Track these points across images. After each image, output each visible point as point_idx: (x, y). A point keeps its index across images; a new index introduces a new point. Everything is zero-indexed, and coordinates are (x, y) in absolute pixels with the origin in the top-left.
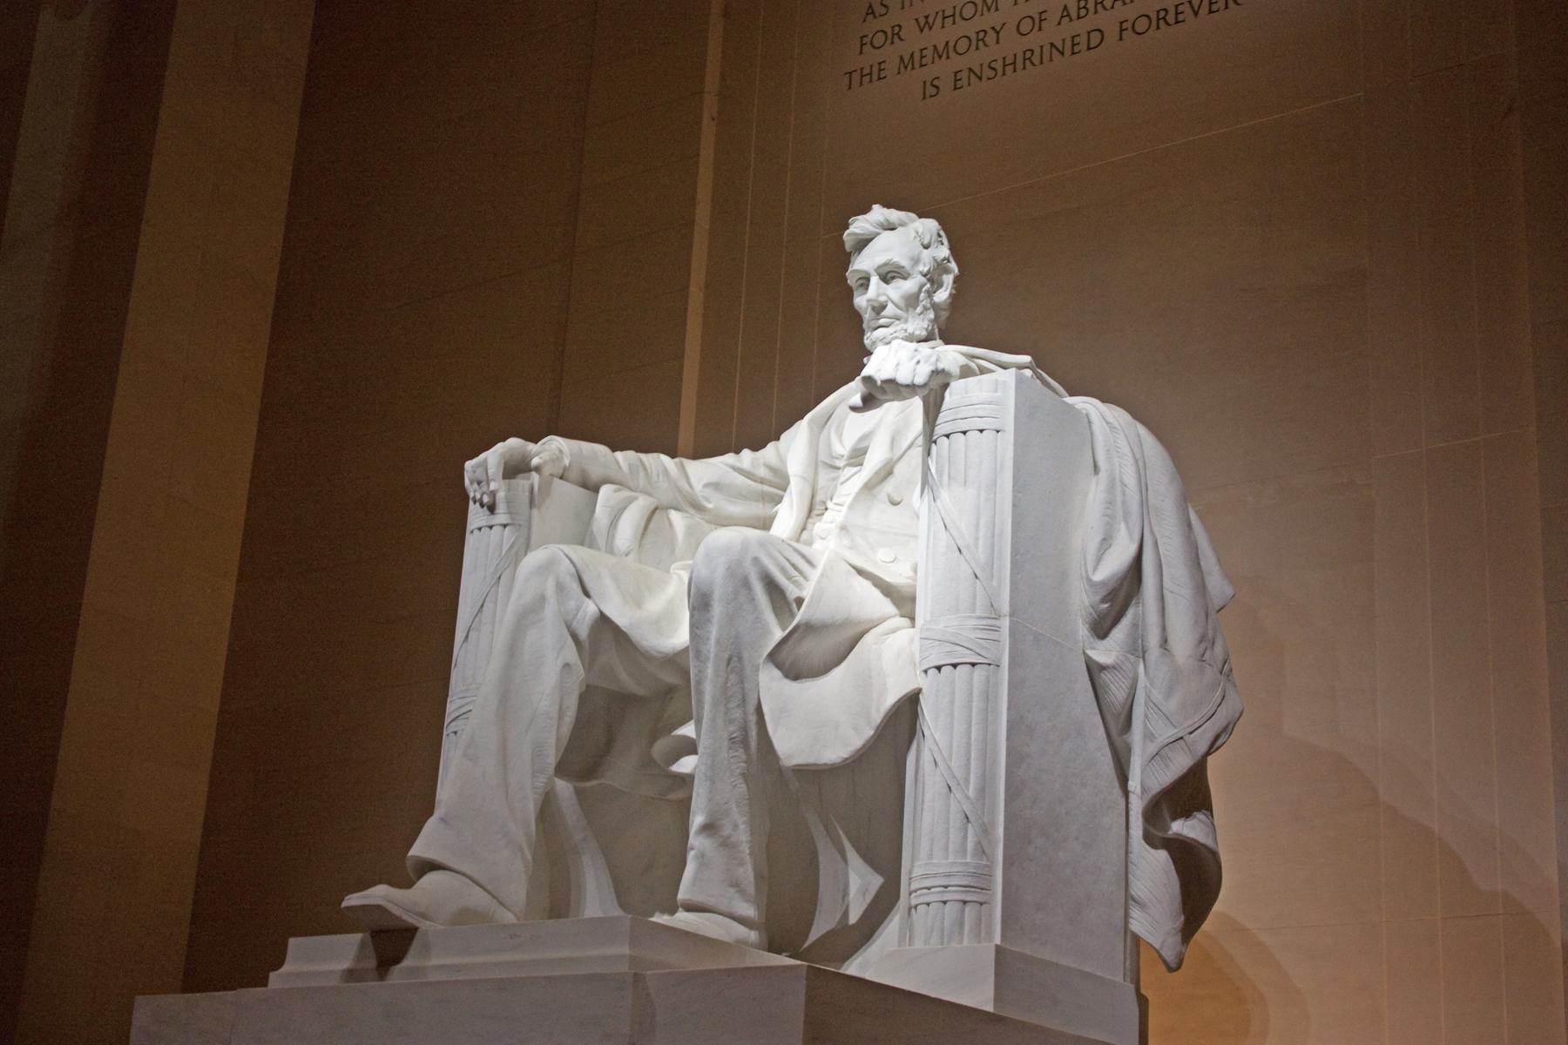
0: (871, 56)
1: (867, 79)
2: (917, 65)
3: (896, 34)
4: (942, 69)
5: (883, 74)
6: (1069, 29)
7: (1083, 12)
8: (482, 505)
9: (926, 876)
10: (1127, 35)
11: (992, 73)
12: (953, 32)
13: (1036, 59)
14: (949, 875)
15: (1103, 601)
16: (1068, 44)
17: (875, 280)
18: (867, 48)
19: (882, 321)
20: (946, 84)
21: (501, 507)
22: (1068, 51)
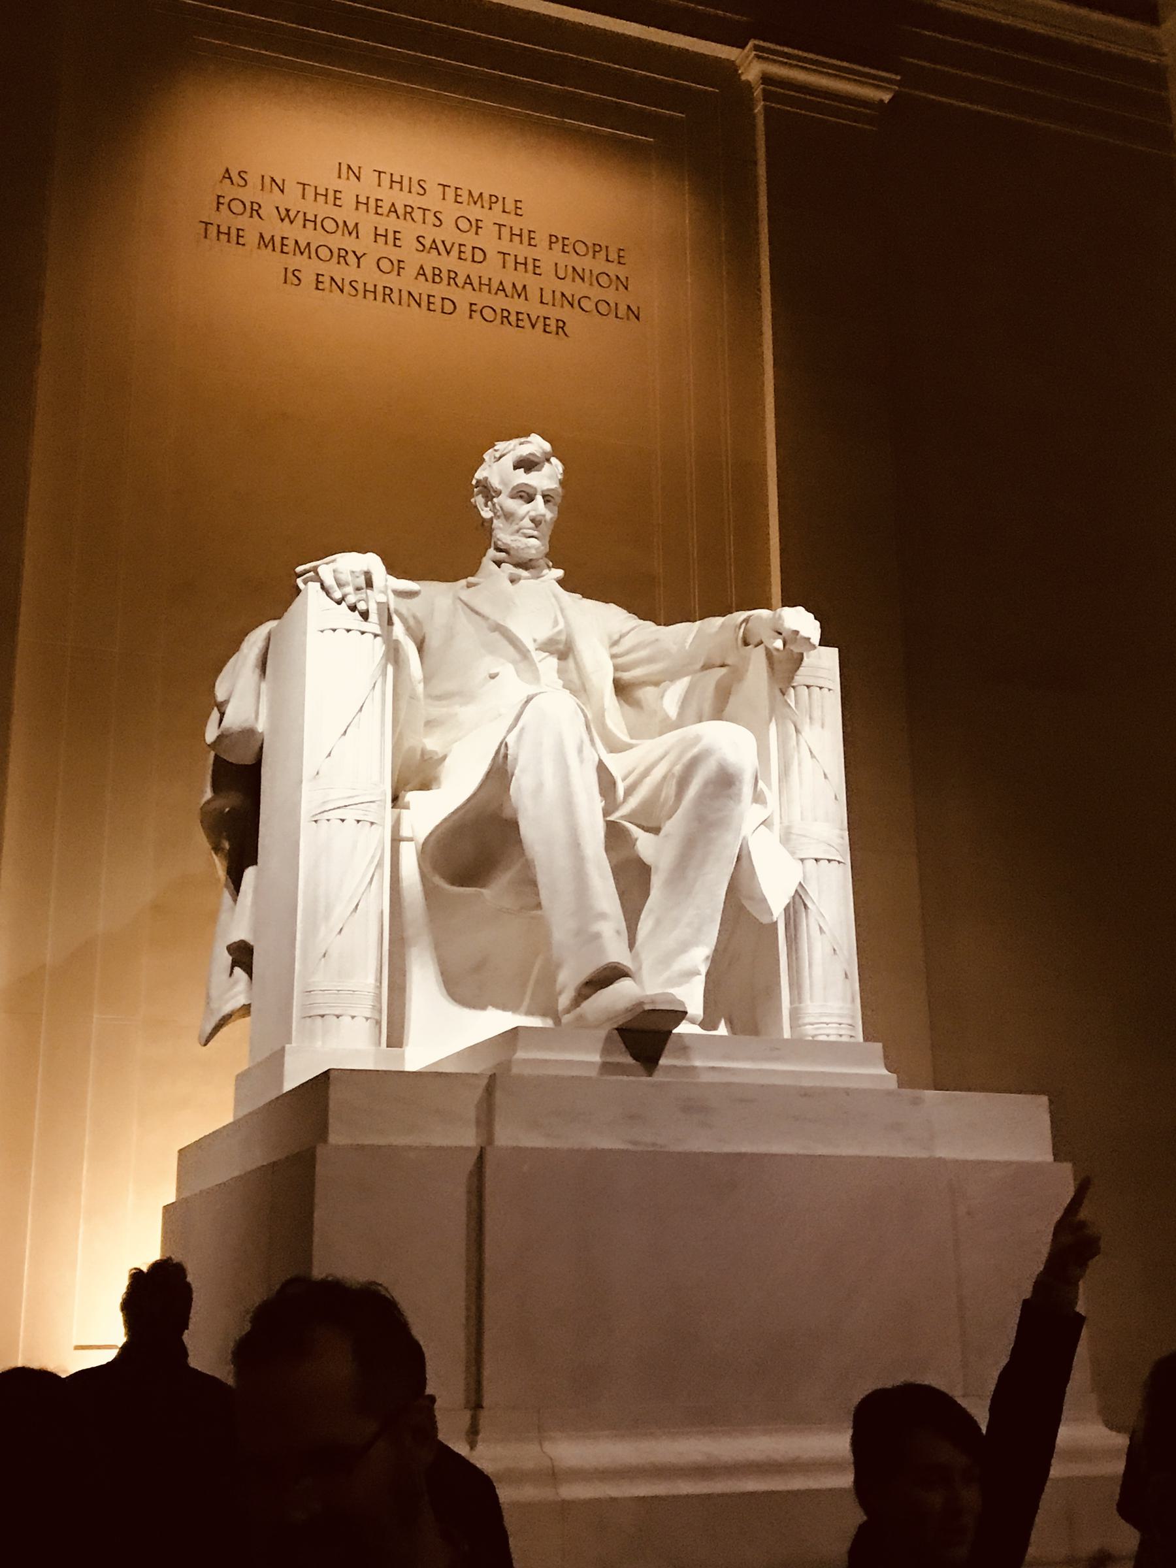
1: (223, 237)
3: (255, 210)
4: (308, 267)
5: (241, 241)
7: (437, 279)
8: (353, 608)
9: (821, 1015)
10: (476, 316)
11: (354, 292)
12: (316, 238)
13: (395, 296)
14: (840, 1016)
16: (425, 298)
19: (535, 533)
20: (308, 278)
21: (373, 616)
22: (424, 303)
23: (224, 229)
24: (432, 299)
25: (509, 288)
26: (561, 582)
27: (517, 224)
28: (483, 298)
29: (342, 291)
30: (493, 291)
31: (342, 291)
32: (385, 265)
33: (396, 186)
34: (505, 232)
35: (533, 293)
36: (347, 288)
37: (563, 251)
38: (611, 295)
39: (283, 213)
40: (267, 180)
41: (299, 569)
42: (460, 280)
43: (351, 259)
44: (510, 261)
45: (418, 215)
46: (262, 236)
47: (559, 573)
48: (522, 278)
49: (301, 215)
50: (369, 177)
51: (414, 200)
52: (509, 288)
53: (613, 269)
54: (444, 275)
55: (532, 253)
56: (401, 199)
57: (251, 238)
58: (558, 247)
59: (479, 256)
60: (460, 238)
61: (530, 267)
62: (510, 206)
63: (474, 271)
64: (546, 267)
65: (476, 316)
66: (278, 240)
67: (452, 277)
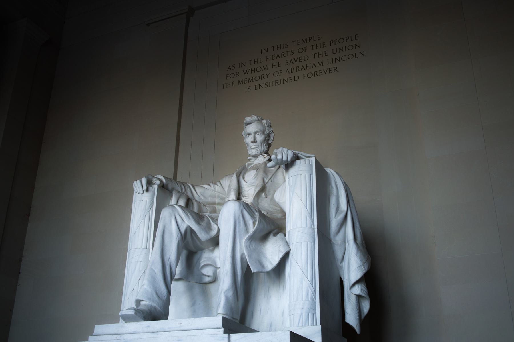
7: (293, 71)
13: (279, 83)
15: (337, 226)
17: (253, 135)
18: (229, 78)
22: (288, 81)
23: (229, 84)
32: (276, 74)
36: (265, 86)
39: (245, 71)
40: (241, 64)
42: (300, 69)
43: (266, 77)
44: (317, 55)
45: (286, 55)
47: (268, 158)
54: (295, 69)
58: (333, 44)
59: (306, 58)
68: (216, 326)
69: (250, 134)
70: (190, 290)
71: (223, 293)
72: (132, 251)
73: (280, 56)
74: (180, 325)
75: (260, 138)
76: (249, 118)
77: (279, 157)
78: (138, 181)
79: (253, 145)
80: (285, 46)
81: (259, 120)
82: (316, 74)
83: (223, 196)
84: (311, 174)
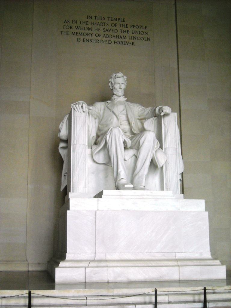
0: (65, 30)
1: (65, 34)
2: (76, 34)
4: (82, 38)
6: (104, 39)
7: (108, 37)
10: (116, 43)
13: (99, 41)
16: (105, 41)
18: (65, 28)
22: (105, 42)
24: (107, 41)
25: (122, 37)
26: (127, 101)
27: (124, 23)
28: (117, 40)
29: (88, 41)
30: (119, 37)
31: (88, 41)
32: (97, 35)
33: (99, 19)
34: (121, 25)
35: (127, 38)
36: (90, 41)
37: (134, 28)
38: (144, 36)
41: (71, 105)
42: (112, 37)
43: (90, 35)
44: (123, 31)
45: (103, 24)
46: (72, 32)
47: (126, 99)
48: (125, 34)
49: (80, 27)
50: (93, 18)
51: (102, 21)
52: (122, 37)
53: (144, 30)
54: (109, 36)
55: (127, 29)
56: (100, 21)
57: (71, 33)
60: (112, 28)
61: (127, 32)
62: (122, 20)
63: (115, 34)
64: (130, 32)
65: (116, 43)
66: (76, 33)
67: (111, 36)
68: (170, 195)
69: (119, 83)
70: (106, 170)
71: (144, 176)
72: (78, 145)
73: (100, 23)
74: (152, 193)
75: (123, 87)
76: (120, 74)
77: (167, 112)
78: (80, 106)
79: (120, 90)
80: (103, 19)
81: (123, 77)
82: (121, 43)
83: (98, 114)
84: (175, 121)
